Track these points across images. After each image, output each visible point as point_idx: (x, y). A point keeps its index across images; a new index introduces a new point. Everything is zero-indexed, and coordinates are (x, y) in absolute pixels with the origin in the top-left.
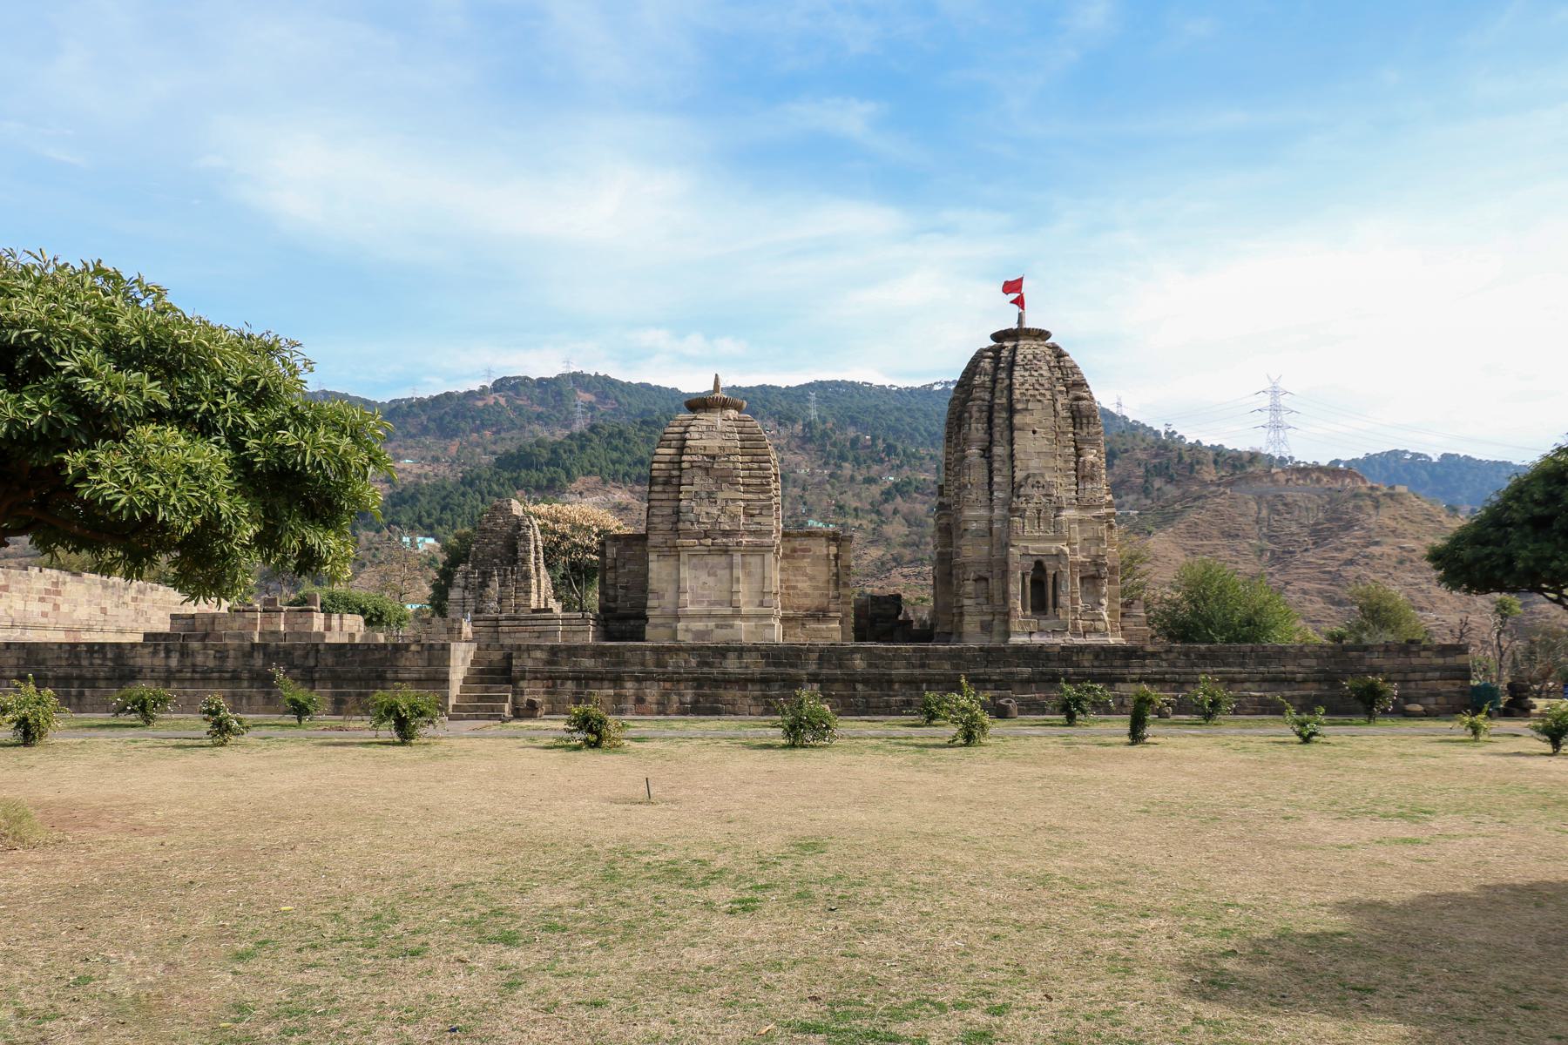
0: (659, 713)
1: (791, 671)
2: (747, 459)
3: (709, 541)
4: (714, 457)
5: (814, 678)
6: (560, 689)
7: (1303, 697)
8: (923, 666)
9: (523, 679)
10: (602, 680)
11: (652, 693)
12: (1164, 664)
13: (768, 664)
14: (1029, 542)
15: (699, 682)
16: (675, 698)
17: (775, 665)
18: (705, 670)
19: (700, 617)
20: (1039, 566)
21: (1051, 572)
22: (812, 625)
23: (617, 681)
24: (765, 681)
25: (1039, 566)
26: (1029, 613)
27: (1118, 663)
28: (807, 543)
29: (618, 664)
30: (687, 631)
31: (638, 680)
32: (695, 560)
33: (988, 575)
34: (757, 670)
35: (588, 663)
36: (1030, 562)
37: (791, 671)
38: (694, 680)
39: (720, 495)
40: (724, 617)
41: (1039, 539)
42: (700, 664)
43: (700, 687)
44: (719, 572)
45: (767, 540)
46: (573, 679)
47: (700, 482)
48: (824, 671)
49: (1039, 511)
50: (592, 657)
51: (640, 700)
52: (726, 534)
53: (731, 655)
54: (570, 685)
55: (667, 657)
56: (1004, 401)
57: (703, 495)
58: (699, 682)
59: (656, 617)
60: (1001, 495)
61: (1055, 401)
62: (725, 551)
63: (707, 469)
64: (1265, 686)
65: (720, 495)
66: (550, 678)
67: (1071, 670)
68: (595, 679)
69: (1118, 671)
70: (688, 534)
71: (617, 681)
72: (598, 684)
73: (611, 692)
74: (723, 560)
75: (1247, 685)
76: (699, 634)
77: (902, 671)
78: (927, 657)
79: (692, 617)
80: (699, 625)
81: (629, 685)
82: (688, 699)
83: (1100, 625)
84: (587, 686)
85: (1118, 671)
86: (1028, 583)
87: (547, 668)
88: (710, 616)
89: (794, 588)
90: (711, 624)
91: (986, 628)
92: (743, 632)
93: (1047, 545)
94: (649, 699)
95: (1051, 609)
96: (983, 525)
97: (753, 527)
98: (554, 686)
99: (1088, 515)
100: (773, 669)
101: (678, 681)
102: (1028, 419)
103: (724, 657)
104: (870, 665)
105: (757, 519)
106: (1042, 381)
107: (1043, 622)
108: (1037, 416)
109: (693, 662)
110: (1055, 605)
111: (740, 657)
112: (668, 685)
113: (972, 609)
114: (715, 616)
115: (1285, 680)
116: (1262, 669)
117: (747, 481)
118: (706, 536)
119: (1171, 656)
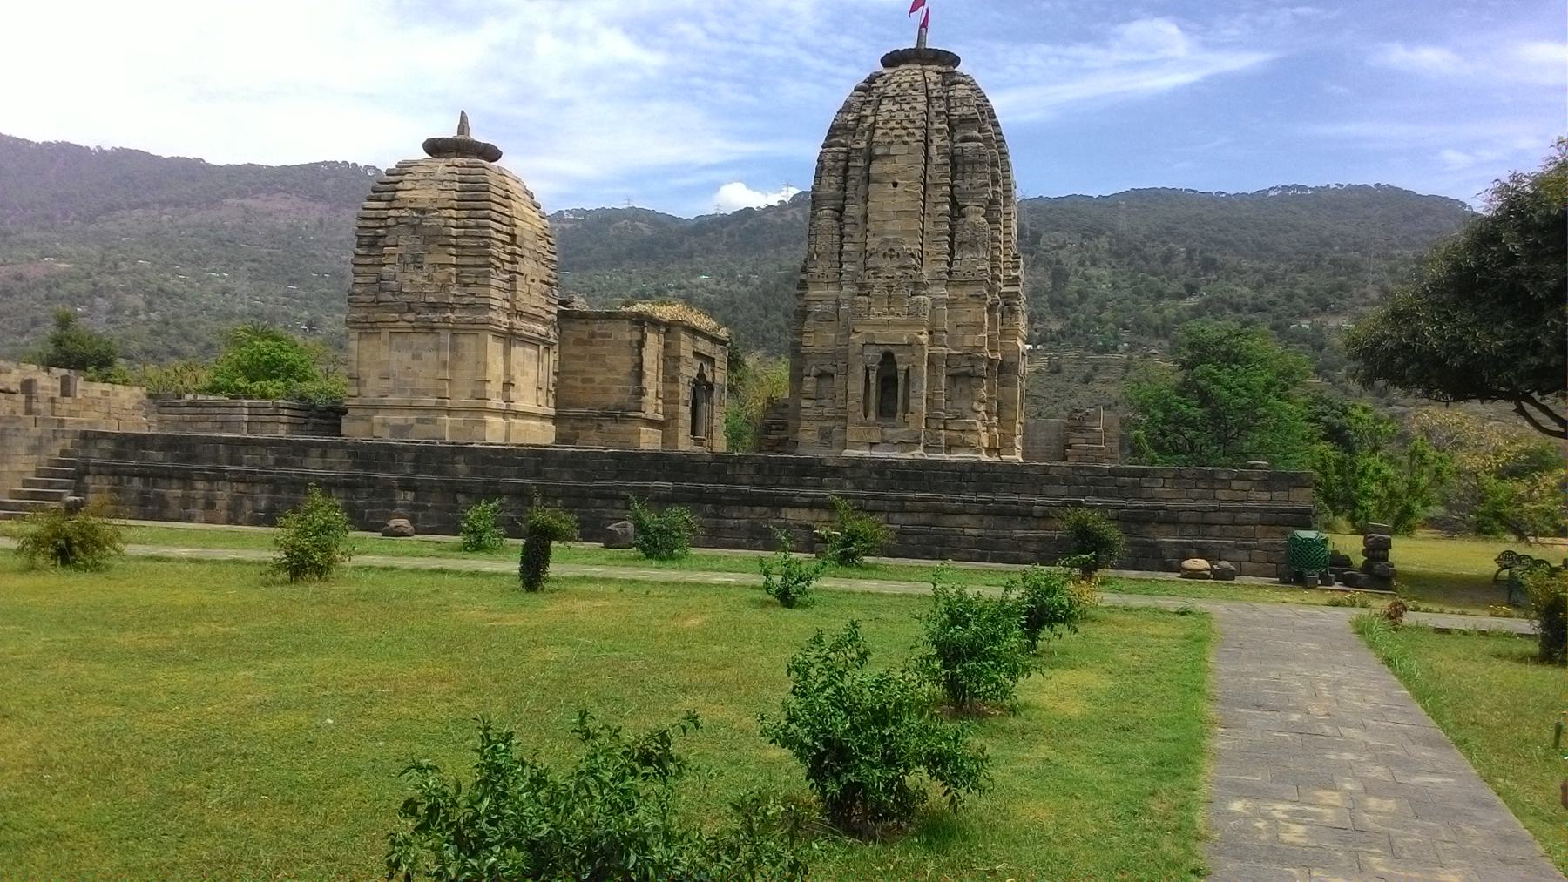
0: (229, 522)
1: (381, 475)
2: (463, 213)
3: (410, 316)
4: (423, 211)
5: (407, 485)
6: (126, 486)
7: (1041, 539)
8: (538, 474)
9: (88, 474)
10: (170, 477)
11: (223, 494)
12: (848, 483)
13: (354, 466)
14: (884, 326)
15: (275, 484)
16: (248, 503)
17: (365, 467)
18: (283, 470)
19: (402, 408)
20: (888, 358)
21: (902, 367)
22: (609, 426)
23: (186, 479)
24: (350, 486)
25: (888, 358)
26: (872, 417)
27: (785, 480)
28: (608, 326)
29: (189, 459)
30: (384, 425)
31: (207, 479)
32: (398, 339)
33: (832, 370)
34: (342, 473)
35: (156, 457)
36: (873, 355)
37: (381, 475)
38: (270, 481)
39: (428, 259)
40: (428, 409)
41: (888, 324)
42: (278, 463)
43: (277, 490)
44: (425, 354)
45: (482, 317)
46: (140, 475)
47: (407, 242)
48: (419, 477)
49: (890, 287)
50: (161, 449)
51: (210, 504)
52: (433, 307)
53: (315, 452)
54: (137, 483)
55: (242, 451)
56: (863, 144)
57: (409, 260)
58: (275, 484)
59: (356, 407)
60: (851, 268)
61: (927, 143)
62: (431, 330)
63: (413, 226)
64: (987, 521)
65: (428, 259)
66: (114, 474)
67: (722, 487)
68: (162, 477)
69: (785, 491)
70: (390, 308)
71: (186, 479)
72: (165, 483)
73: (179, 492)
74: (429, 340)
75: (964, 519)
76: (399, 430)
77: (512, 480)
78: (544, 462)
79: (392, 408)
80: (397, 419)
81: (200, 485)
82: (263, 504)
83: (971, 438)
84: (155, 485)
85: (785, 491)
86: (873, 381)
87: (113, 462)
88: (411, 408)
89: (591, 381)
90: (412, 417)
91: (825, 436)
92: (495, 432)
93: (898, 332)
94: (220, 504)
95: (900, 414)
96: (830, 307)
97: (466, 300)
98: (120, 483)
99: (964, 293)
100: (361, 473)
101: (253, 483)
102: (889, 167)
103: (306, 455)
104: (475, 471)
105: (470, 290)
106: (913, 116)
107: (888, 431)
108: (901, 163)
109: (271, 459)
110: (906, 409)
111: (323, 455)
112: (242, 487)
113: (809, 413)
114: (417, 408)
115: (1016, 514)
116: (984, 497)
117: (462, 241)
118: (410, 310)
119: (859, 473)
